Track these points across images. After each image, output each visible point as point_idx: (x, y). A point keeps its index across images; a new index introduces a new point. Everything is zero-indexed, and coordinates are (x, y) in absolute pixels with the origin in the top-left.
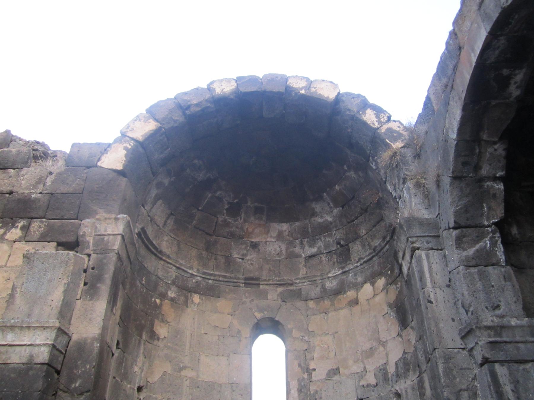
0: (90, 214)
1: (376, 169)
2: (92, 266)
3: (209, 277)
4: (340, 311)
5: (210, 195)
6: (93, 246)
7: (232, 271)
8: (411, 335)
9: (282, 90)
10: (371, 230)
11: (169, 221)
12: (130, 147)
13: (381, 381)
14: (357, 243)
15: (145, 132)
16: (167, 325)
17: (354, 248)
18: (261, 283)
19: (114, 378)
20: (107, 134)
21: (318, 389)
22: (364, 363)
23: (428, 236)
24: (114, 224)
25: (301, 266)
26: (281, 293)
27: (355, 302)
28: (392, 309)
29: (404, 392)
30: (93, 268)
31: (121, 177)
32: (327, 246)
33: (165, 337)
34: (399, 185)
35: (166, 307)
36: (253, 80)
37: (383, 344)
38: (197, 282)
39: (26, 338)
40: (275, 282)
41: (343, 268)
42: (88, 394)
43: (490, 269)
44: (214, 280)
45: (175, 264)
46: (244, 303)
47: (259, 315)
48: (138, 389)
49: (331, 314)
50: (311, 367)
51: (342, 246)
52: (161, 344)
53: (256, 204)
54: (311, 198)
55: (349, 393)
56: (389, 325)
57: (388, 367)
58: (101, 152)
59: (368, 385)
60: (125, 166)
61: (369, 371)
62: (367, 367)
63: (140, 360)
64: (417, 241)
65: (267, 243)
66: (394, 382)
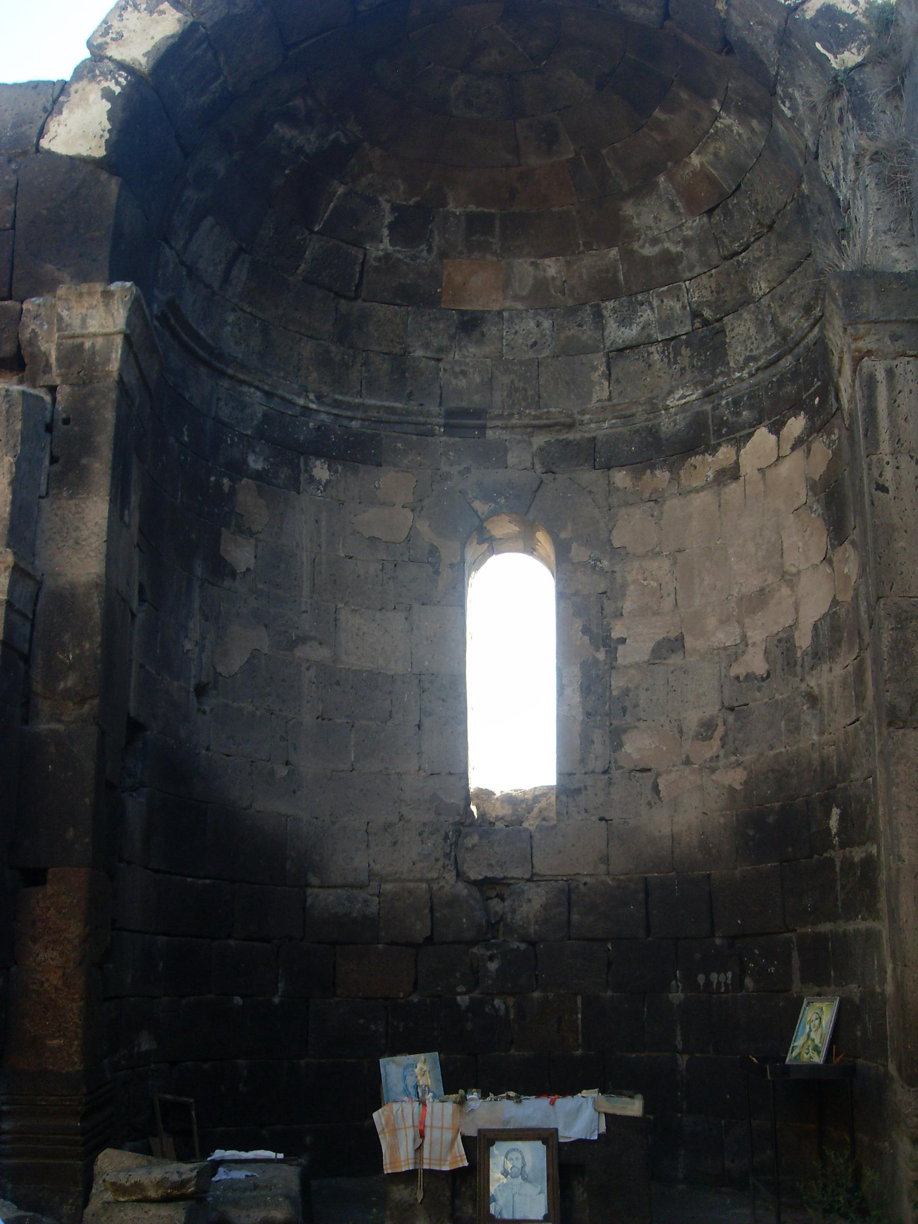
1: (792, 120)
2: (64, 416)
3: (349, 414)
4: (692, 495)
5: (341, 190)
6: (60, 367)
7: (411, 393)
8: (850, 563)
10: (781, 283)
11: (235, 272)
12: (117, 90)
13: (779, 667)
14: (746, 316)
15: (153, 43)
16: (252, 541)
17: (736, 331)
18: (490, 424)
19: (142, 666)
20: (55, 57)
21: (630, 685)
22: (742, 625)
23: (896, 321)
24: (102, 308)
25: (595, 376)
26: (541, 449)
27: (732, 473)
28: (815, 494)
29: (825, 693)
30: (66, 422)
33: (248, 569)
34: (845, 172)
35: (247, 497)
37: (789, 579)
38: (319, 427)
40: (526, 421)
41: (704, 384)
42: (96, 701)
44: (363, 420)
45: (260, 384)
46: (447, 477)
48: (195, 690)
49: (672, 504)
50: (615, 635)
51: (706, 323)
53: (472, 208)
54: (626, 188)
55: (704, 694)
56: (808, 533)
57: (796, 635)
58: (45, 110)
59: (749, 677)
60: (111, 145)
61: (754, 644)
62: (749, 634)
63: (195, 624)
64: (868, 333)
65: (505, 314)
66: (807, 669)
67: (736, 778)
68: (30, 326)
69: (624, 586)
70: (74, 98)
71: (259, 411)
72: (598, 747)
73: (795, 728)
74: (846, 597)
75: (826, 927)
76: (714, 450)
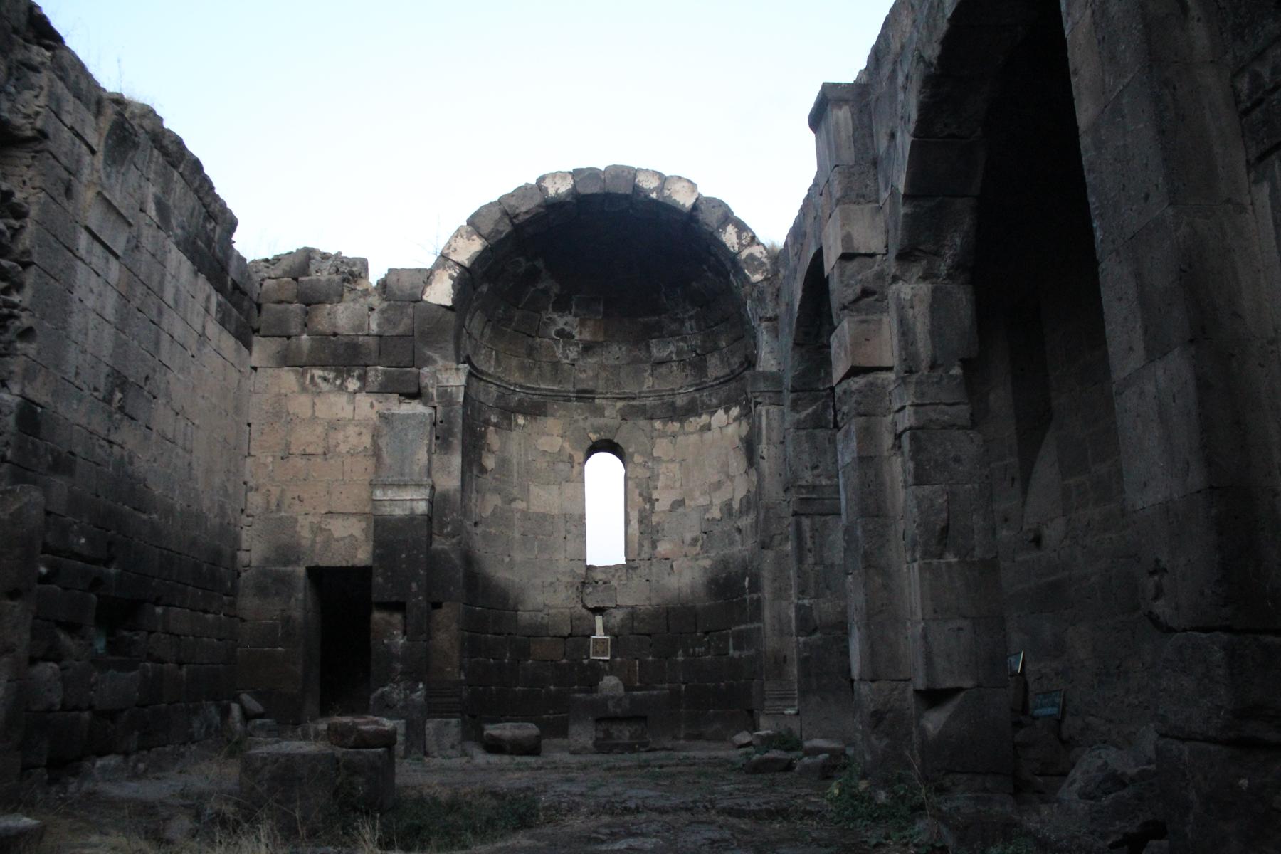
0: (428, 361)
9: (629, 192)
25: (646, 375)
27: (708, 427)
31: (450, 313)
32: (679, 352)
36: (593, 174)
37: (731, 478)
39: (407, 495)
43: (817, 431)
46: (576, 421)
47: (594, 437)
49: (680, 439)
52: (488, 477)
60: (453, 300)
63: (474, 495)
67: (707, 563)
68: (426, 381)
69: (658, 475)
70: (437, 277)
71: (495, 394)
72: (647, 547)
73: (732, 543)
74: (753, 490)
75: (743, 627)
76: (700, 415)
